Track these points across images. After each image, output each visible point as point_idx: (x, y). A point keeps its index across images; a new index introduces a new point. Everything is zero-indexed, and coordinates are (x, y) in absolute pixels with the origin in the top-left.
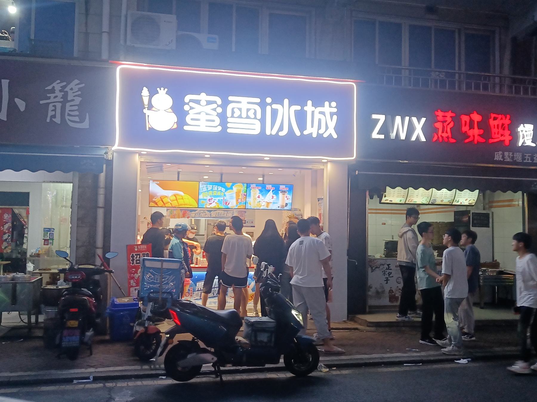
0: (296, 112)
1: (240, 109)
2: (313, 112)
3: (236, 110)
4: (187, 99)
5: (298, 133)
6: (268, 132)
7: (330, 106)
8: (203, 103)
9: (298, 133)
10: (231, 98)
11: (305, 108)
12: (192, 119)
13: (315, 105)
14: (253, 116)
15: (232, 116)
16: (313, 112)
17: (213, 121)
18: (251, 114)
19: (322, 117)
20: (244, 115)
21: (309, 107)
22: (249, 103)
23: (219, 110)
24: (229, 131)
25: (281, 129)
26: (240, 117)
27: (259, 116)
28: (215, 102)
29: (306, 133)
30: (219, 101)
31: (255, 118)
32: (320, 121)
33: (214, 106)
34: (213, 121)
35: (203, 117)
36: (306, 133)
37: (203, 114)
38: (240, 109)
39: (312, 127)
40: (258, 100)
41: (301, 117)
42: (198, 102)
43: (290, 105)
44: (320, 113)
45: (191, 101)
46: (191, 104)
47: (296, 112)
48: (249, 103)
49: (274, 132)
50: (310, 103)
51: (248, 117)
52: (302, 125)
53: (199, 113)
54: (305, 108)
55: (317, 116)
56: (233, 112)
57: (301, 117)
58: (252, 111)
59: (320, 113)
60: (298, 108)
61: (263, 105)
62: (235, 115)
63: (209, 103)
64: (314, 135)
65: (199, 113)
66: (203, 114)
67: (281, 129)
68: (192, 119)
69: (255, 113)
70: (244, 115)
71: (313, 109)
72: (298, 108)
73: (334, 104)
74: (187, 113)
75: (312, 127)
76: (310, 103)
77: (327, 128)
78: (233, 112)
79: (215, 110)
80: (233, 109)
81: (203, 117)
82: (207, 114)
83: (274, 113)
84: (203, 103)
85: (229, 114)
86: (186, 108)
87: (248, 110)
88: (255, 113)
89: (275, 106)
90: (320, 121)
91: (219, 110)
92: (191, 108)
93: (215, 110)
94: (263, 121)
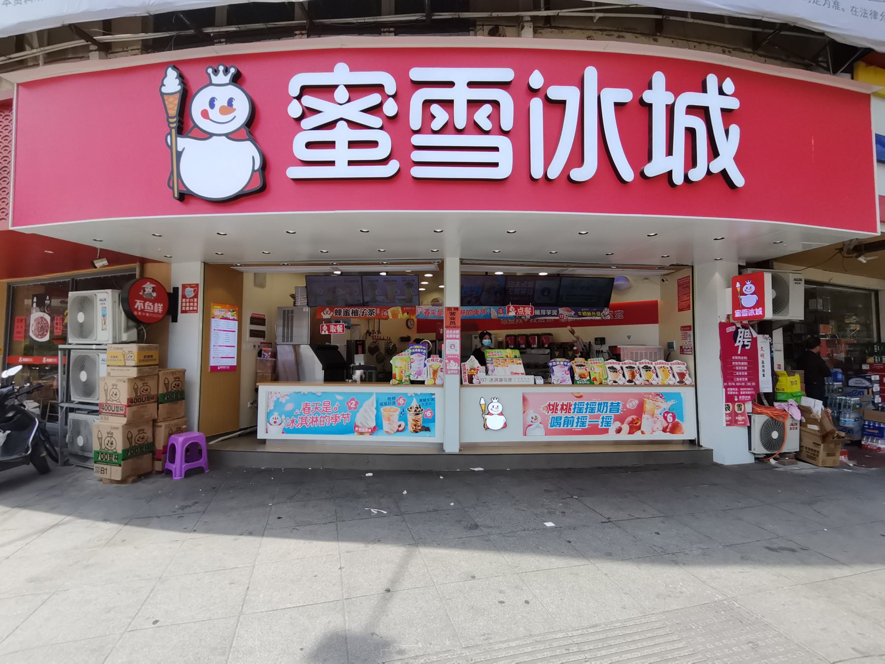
0: (618, 106)
1: (448, 104)
2: (670, 110)
3: (435, 109)
5: (627, 173)
6: (537, 172)
7: (721, 92)
8: (341, 94)
10: (417, 74)
11: (647, 96)
12: (310, 145)
13: (675, 88)
16: (670, 110)
17: (374, 144)
18: (482, 116)
20: (460, 122)
22: (472, 85)
24: (418, 172)
25: (577, 157)
26: (448, 128)
27: (507, 122)
28: (378, 88)
30: (391, 87)
32: (691, 133)
33: (374, 99)
34: (374, 144)
35: (342, 134)
36: (652, 170)
37: (342, 125)
38: (448, 104)
39: (669, 152)
40: (506, 74)
43: (602, 84)
44: (691, 110)
45: (305, 90)
46: (309, 101)
47: (618, 106)
48: (472, 85)
49: (554, 172)
50: (659, 79)
53: (330, 125)
55: (683, 121)
56: (428, 117)
58: (487, 109)
59: (691, 110)
60: (625, 95)
62: (436, 125)
63: (355, 90)
64: (678, 179)
65: (330, 125)
66: (342, 125)
67: (577, 157)
68: (310, 145)
69: (495, 117)
70: (460, 122)
71: (669, 98)
72: (625, 95)
73: (729, 86)
75: (669, 152)
76: (659, 79)
77: (714, 153)
78: (428, 117)
80: (427, 103)
81: (342, 134)
82: (353, 125)
84: (341, 94)
85: (415, 121)
87: (474, 105)
88: (495, 117)
90: (691, 133)
91: (391, 108)
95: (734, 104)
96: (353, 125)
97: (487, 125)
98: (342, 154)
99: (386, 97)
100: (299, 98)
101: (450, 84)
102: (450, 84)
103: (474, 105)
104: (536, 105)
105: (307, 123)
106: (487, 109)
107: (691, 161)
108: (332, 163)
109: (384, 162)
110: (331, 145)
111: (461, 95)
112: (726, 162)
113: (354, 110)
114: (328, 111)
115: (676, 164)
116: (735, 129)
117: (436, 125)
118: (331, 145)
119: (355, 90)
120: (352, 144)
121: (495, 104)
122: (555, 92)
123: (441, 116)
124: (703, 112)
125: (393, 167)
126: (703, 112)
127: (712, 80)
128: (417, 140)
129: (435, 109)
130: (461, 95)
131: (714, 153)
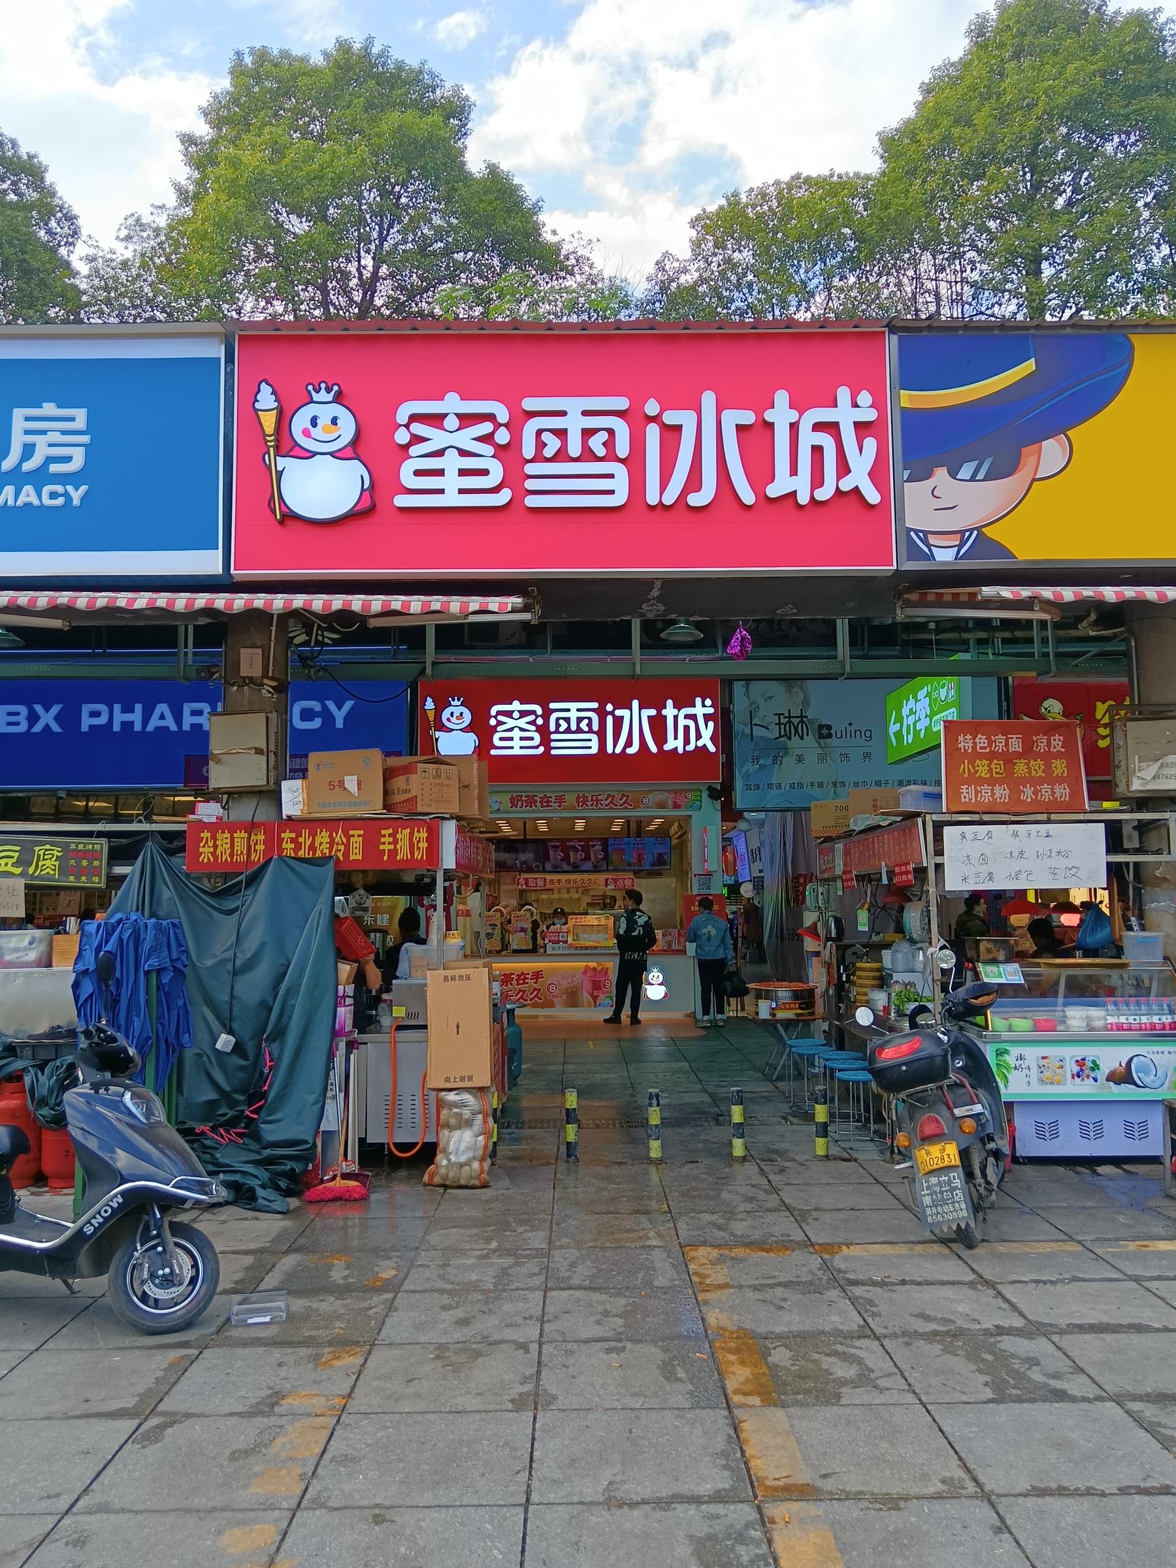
2: (676, 718)
3: (561, 722)
4: (494, 710)
5: (653, 748)
6: (610, 750)
7: (704, 706)
8: (516, 715)
9: (653, 748)
10: (553, 706)
11: (664, 712)
12: (501, 739)
13: (678, 706)
14: (586, 729)
15: (557, 731)
16: (676, 718)
17: (532, 739)
19: (691, 724)
20: (574, 727)
21: (669, 711)
22: (578, 710)
23: (540, 721)
24: (553, 752)
26: (568, 731)
27: (595, 727)
28: (533, 712)
29: (667, 747)
30: (539, 711)
31: (591, 731)
32: (687, 728)
33: (531, 718)
34: (532, 739)
35: (516, 734)
36: (667, 747)
37: (516, 730)
38: (567, 720)
39: (676, 738)
40: (595, 705)
41: (658, 726)
42: (509, 714)
44: (687, 717)
45: (499, 713)
46: (501, 718)
48: (578, 710)
49: (618, 750)
51: (579, 730)
52: (660, 738)
53: (511, 730)
54: (664, 712)
55: (682, 722)
56: (558, 725)
57: (658, 726)
58: (586, 721)
59: (687, 717)
60: (653, 712)
61: (602, 713)
62: (561, 729)
63: (523, 714)
64: (680, 751)
65: (511, 730)
66: (516, 730)
67: (629, 743)
68: (501, 739)
69: (590, 725)
70: (574, 727)
71: (675, 712)
72: (653, 712)
73: (708, 702)
74: (494, 730)
78: (558, 725)
79: (533, 723)
80: (558, 719)
81: (516, 734)
82: (522, 730)
83: (618, 722)
84: (516, 715)
85: (552, 727)
86: (493, 722)
87: (580, 720)
88: (590, 725)
89: (618, 713)
90: (687, 728)
91: (540, 721)
92: (500, 723)
93: (533, 723)
94: (602, 734)
95: (711, 710)
96: (522, 730)
97: (586, 729)
98: (517, 743)
99: (537, 717)
100: (495, 717)
101: (568, 710)
102: (568, 710)
103: (580, 720)
104: (610, 719)
105: (499, 728)
106: (586, 721)
107: (687, 741)
108: (512, 748)
109: (537, 747)
110: (511, 739)
111: (573, 715)
112: (706, 740)
113: (522, 723)
114: (510, 723)
115: (679, 744)
116: (711, 724)
117: (561, 729)
118: (511, 739)
119: (523, 714)
120: (522, 739)
121: (590, 719)
122: (618, 713)
123: (564, 726)
124: (693, 717)
125: (541, 749)
126: (693, 717)
127: (698, 701)
128: (553, 737)
129: (561, 722)
130: (573, 715)
131: (699, 736)
